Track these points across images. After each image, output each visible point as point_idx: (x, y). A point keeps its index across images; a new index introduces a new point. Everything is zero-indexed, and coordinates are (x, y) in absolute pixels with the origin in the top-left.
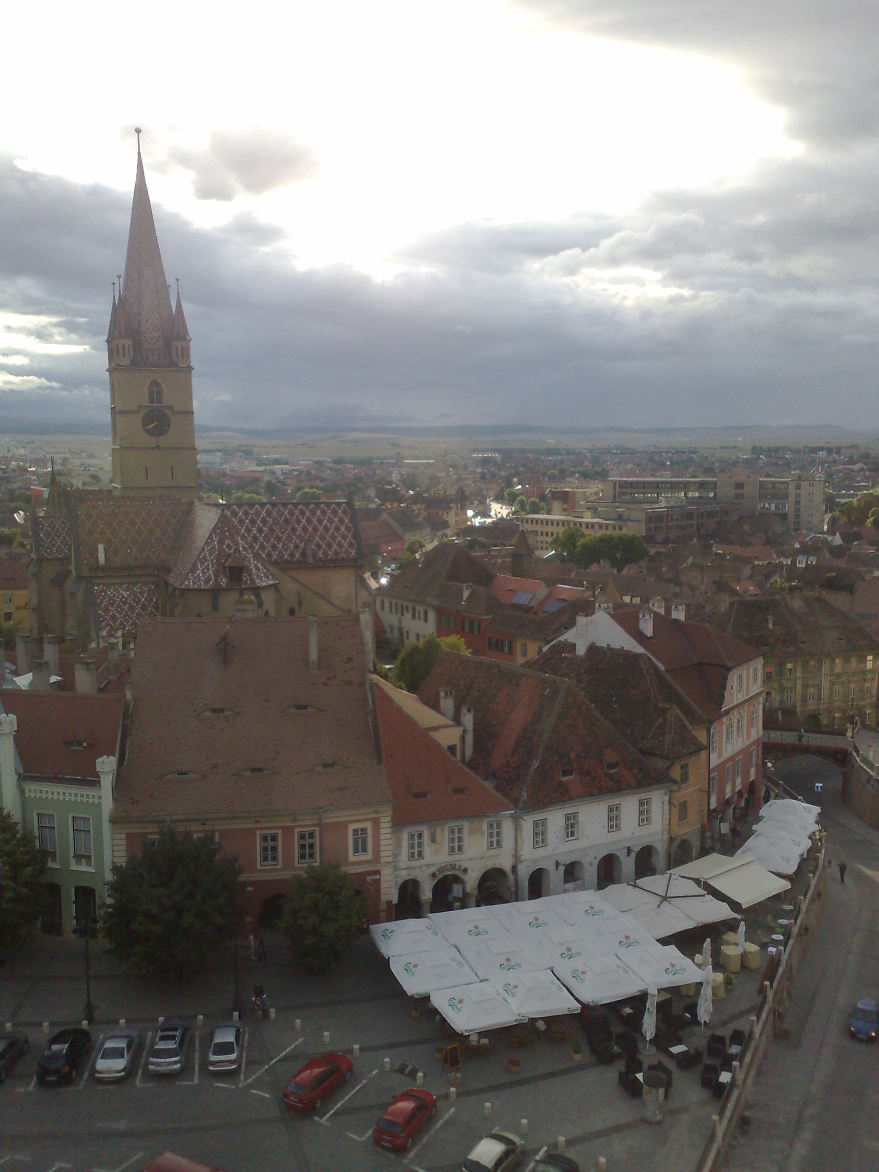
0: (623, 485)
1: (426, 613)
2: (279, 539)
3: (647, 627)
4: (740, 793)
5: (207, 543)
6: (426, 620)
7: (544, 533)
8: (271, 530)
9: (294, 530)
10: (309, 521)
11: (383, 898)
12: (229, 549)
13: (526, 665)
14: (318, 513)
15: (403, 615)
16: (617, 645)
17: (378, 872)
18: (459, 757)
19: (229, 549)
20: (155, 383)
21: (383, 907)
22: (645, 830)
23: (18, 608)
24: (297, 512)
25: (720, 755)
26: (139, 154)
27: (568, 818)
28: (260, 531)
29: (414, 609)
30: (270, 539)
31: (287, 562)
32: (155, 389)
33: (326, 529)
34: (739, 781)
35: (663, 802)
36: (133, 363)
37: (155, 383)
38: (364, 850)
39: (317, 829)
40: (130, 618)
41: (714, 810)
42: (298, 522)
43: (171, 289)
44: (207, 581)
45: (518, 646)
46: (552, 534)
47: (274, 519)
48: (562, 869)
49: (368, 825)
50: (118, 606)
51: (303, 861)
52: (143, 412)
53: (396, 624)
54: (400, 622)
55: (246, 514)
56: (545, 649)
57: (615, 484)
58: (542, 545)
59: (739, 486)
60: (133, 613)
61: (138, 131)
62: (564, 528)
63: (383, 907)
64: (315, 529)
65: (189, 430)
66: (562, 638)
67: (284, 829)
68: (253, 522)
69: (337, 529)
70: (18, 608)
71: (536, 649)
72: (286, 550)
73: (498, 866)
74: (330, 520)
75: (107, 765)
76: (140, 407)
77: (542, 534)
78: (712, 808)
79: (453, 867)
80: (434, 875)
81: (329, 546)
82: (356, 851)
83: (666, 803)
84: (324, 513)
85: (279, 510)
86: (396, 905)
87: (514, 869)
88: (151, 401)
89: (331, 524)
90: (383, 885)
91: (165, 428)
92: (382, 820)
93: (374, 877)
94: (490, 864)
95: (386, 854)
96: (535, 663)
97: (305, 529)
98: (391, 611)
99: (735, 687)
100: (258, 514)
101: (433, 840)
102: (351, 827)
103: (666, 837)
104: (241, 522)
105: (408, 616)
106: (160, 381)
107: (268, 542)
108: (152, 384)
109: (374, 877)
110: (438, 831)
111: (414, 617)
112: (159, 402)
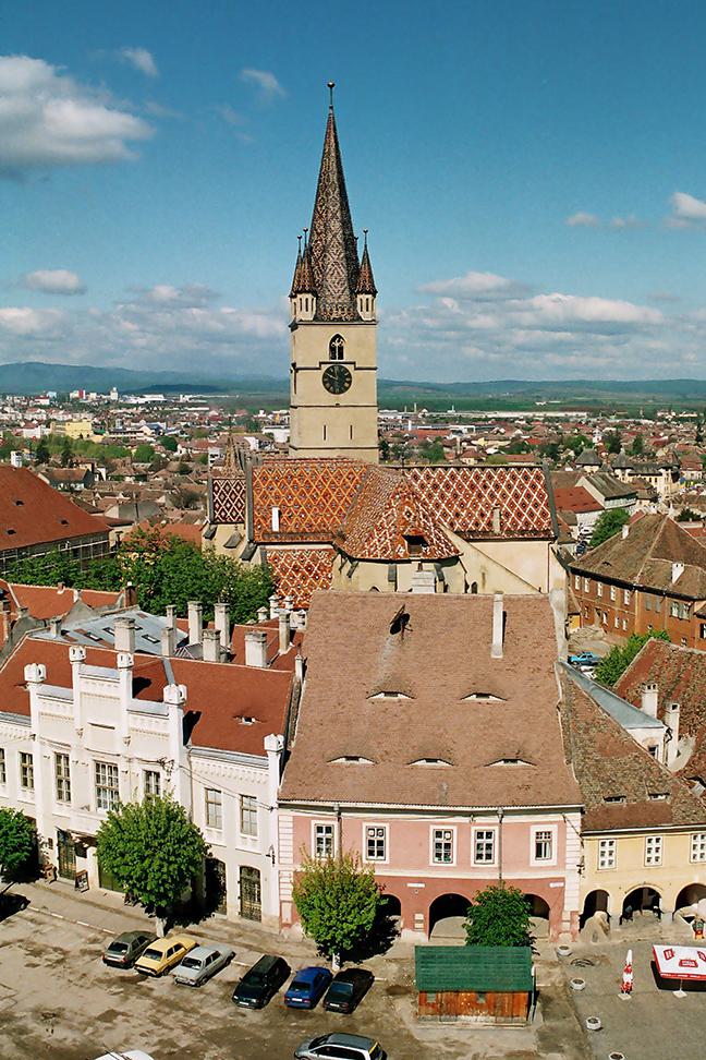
8: (455, 496)
9: (480, 496)
10: (497, 487)
12: (409, 517)
14: (508, 477)
19: (409, 517)
24: (484, 477)
28: (442, 496)
30: (453, 505)
32: (337, 345)
33: (517, 496)
36: (315, 318)
39: (497, 828)
44: (386, 548)
47: (459, 484)
50: (291, 575)
51: (479, 861)
55: (428, 477)
64: (504, 496)
67: (459, 825)
68: (435, 487)
69: (528, 496)
72: (470, 518)
74: (522, 487)
75: (273, 743)
76: (321, 363)
81: (519, 515)
82: (539, 854)
84: (514, 478)
85: (465, 475)
89: (522, 490)
91: (347, 385)
97: (492, 496)
100: (441, 477)
104: (422, 486)
108: (333, 340)
112: (341, 357)
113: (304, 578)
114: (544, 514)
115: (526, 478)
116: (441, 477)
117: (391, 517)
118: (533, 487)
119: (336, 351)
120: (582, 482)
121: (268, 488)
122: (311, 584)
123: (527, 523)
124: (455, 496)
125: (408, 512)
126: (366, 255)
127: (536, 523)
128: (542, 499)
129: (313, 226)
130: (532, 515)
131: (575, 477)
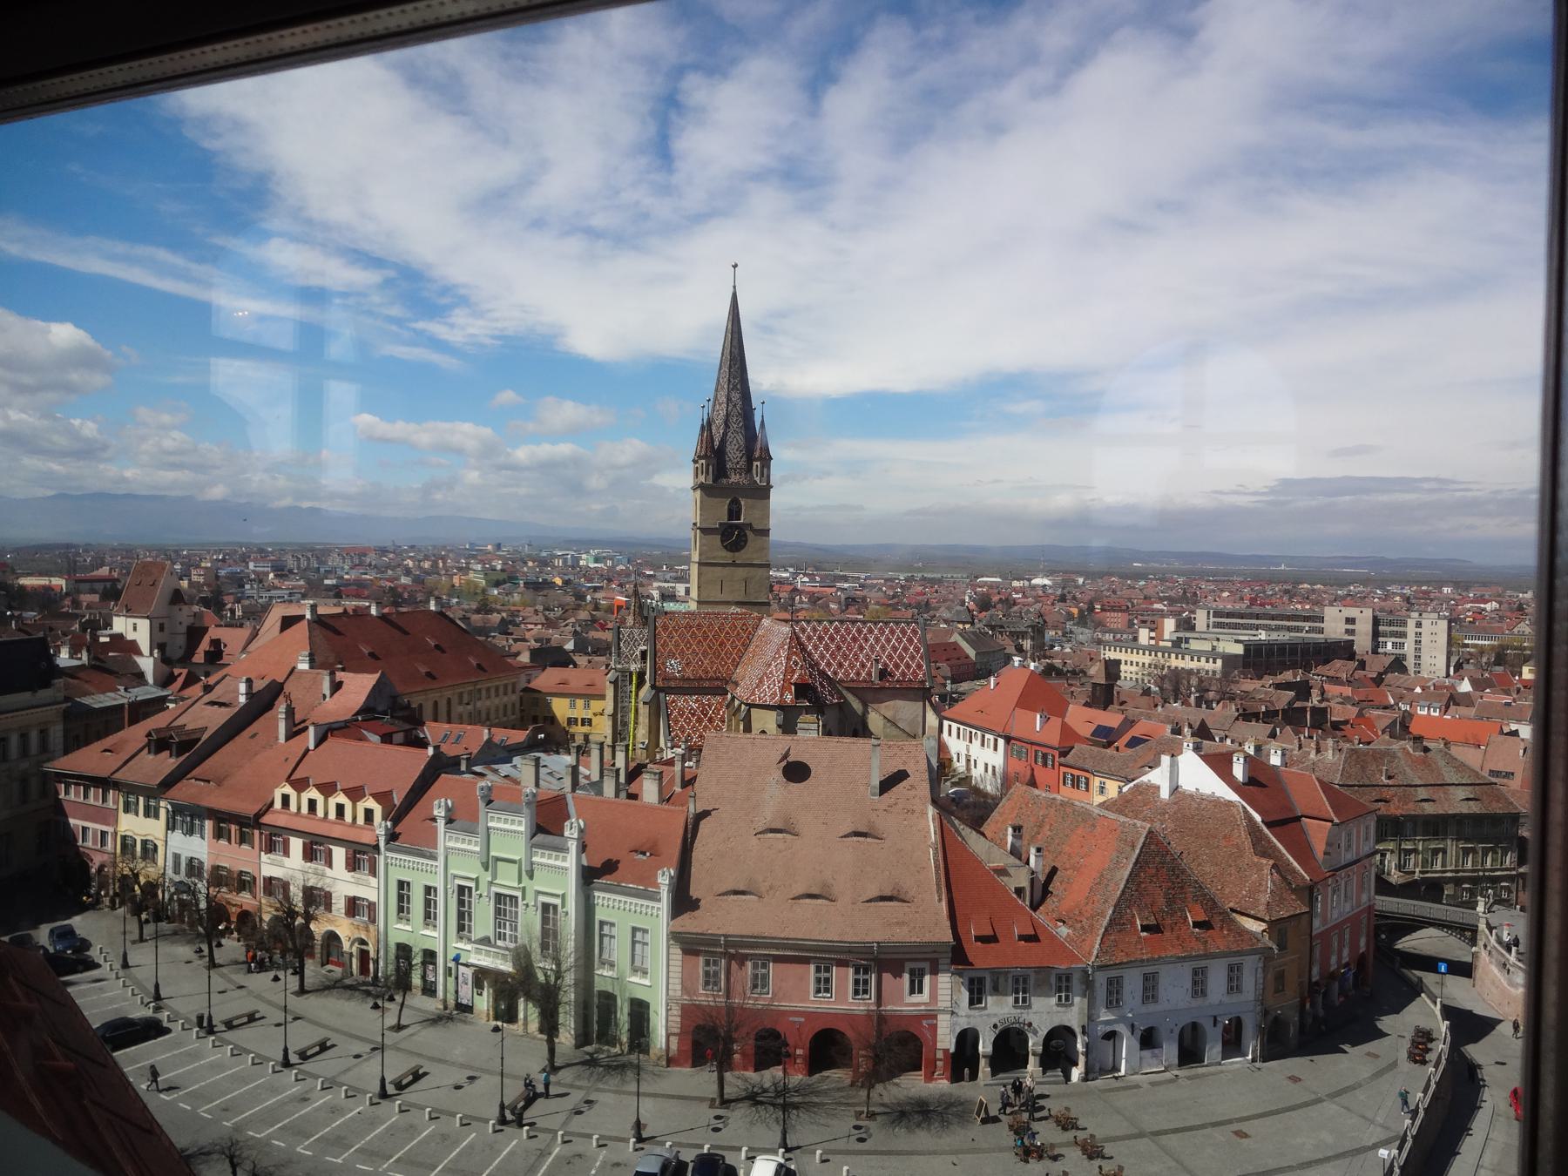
0: (1217, 614)
1: (996, 740)
2: (845, 657)
3: (1238, 771)
4: (1347, 965)
5: (774, 659)
8: (839, 648)
9: (861, 648)
11: (939, 1045)
13: (1102, 805)
15: (971, 742)
16: (1206, 790)
18: (1028, 903)
21: (940, 1055)
22: (1235, 998)
23: (595, 714)
25: (1325, 921)
26: (734, 287)
29: (983, 736)
31: (852, 681)
34: (1346, 952)
35: (1256, 970)
38: (921, 991)
40: (698, 730)
41: (1317, 983)
42: (866, 640)
44: (775, 694)
45: (1096, 782)
46: (1137, 663)
47: (842, 636)
53: (963, 752)
54: (968, 750)
55: (814, 630)
56: (1125, 789)
57: (1209, 612)
59: (1351, 621)
60: (700, 725)
61: (735, 266)
65: (764, 549)
66: (1144, 779)
68: (821, 639)
69: (905, 649)
70: (595, 714)
72: (852, 668)
74: (899, 640)
77: (1126, 664)
78: (1314, 980)
80: (995, 1026)
82: (912, 992)
83: (1260, 970)
84: (892, 632)
86: (953, 1054)
89: (900, 643)
90: (940, 1031)
92: (940, 961)
94: (1057, 1021)
98: (959, 737)
99: (1343, 845)
100: (826, 630)
103: (1259, 1009)
104: (809, 638)
105: (977, 743)
107: (834, 659)
109: (930, 1022)
111: (983, 745)
113: (699, 721)
114: (919, 666)
115: (904, 632)
116: (826, 630)
117: (779, 666)
118: (910, 641)
119: (734, 512)
120: (956, 638)
121: (668, 637)
122: (706, 727)
123: (903, 674)
124: (839, 648)
125: (795, 661)
126: (763, 422)
127: (912, 674)
128: (918, 652)
129: (716, 398)
130: (908, 666)
131: (950, 633)
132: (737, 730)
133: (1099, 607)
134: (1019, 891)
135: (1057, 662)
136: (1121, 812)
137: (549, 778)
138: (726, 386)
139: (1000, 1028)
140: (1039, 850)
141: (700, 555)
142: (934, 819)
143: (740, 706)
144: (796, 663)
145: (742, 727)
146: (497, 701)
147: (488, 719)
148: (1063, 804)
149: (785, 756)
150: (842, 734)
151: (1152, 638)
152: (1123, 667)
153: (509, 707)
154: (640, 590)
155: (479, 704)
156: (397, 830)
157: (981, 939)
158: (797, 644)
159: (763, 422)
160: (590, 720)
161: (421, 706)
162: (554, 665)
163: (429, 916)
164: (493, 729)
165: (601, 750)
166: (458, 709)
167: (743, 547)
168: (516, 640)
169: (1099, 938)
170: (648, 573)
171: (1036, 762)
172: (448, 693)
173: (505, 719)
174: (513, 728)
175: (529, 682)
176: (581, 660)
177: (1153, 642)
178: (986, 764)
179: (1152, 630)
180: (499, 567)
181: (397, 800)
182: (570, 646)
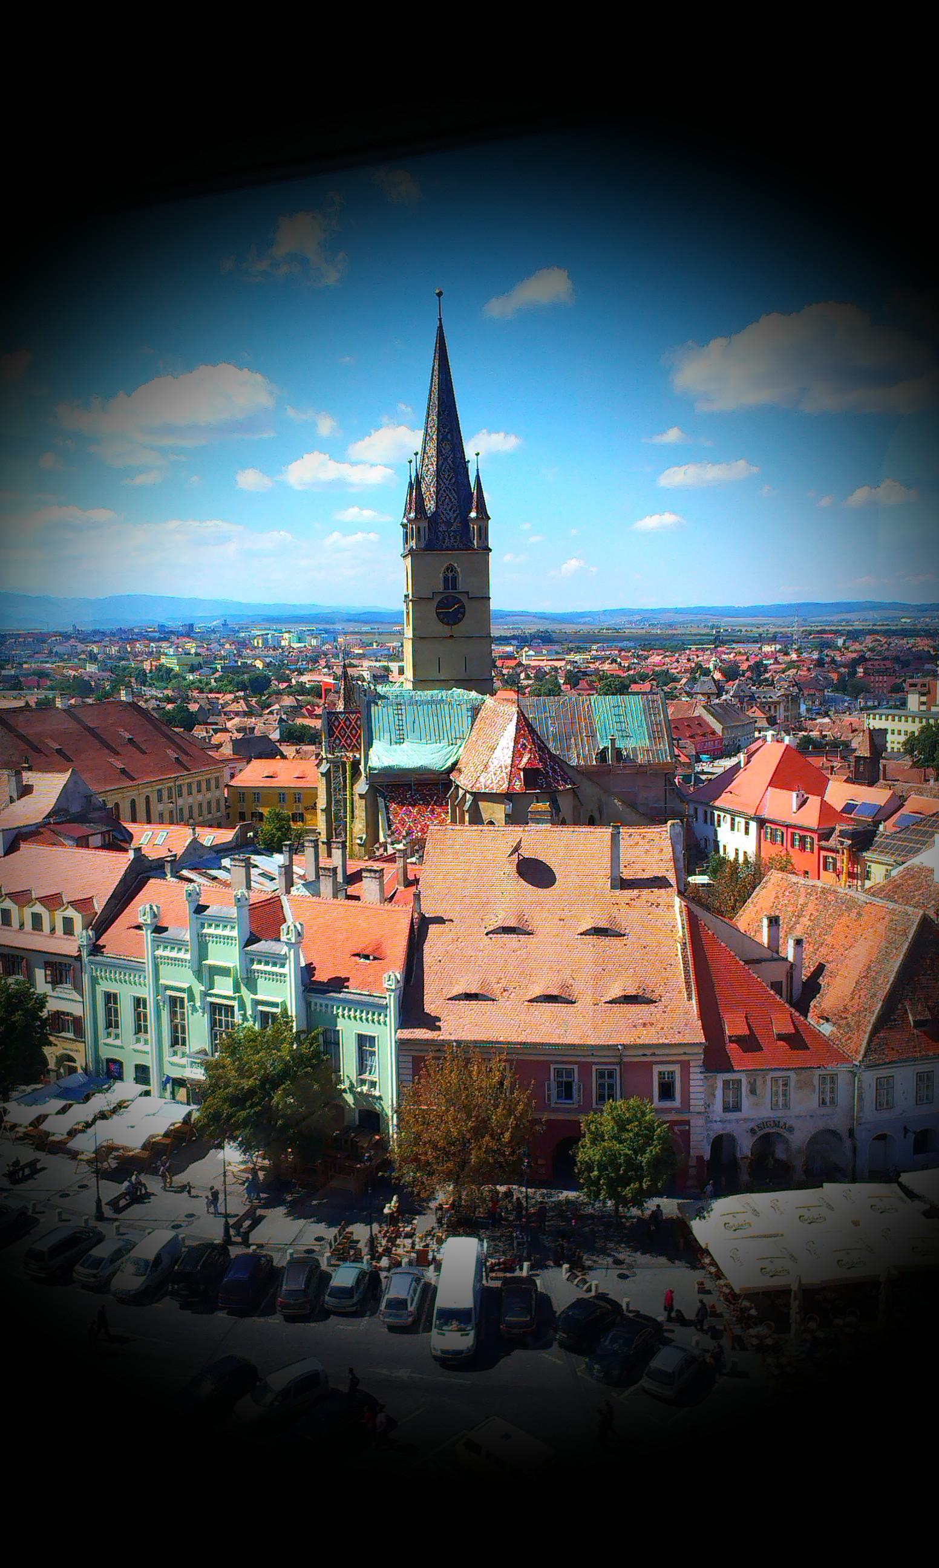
1: (747, 824)
6: (747, 832)
7: (896, 732)
11: (693, 1153)
12: (524, 749)
17: (687, 1123)
20: (450, 568)
21: (693, 1162)
23: (306, 809)
27: (920, 1077)
29: (733, 820)
32: (450, 575)
37: (450, 568)
39: (617, 1068)
43: (470, 466)
48: (911, 1137)
49: (676, 1068)
52: (438, 599)
56: (894, 873)
58: (893, 745)
62: (920, 725)
63: (693, 1162)
70: (306, 809)
71: (884, 872)
73: (832, 1127)
77: (893, 733)
79: (776, 1124)
80: (752, 1131)
87: (851, 1132)
88: (446, 587)
91: (460, 616)
93: (682, 1128)
95: (697, 1100)
96: (882, 889)
98: (706, 822)
101: (753, 1091)
102: (656, 1069)
106: (456, 565)
108: (448, 569)
109: (682, 1128)
110: (759, 1083)
111: (733, 829)
112: (454, 587)
119: (450, 581)
120: (700, 711)
126: (478, 478)
131: (692, 706)
132: (462, 821)
133: (862, 670)
134: (776, 986)
135: (815, 734)
136: (889, 898)
137: (262, 879)
138: (435, 437)
139: (760, 1133)
140: (798, 942)
141: (414, 630)
142: (681, 912)
143: (464, 795)
144: (524, 747)
145: (467, 818)
146: (200, 797)
147: (191, 817)
148: (824, 891)
149: (516, 849)
150: (576, 823)
151: (923, 703)
152: (889, 737)
153: (214, 805)
154: (350, 671)
155: (180, 801)
156: (101, 942)
157: (738, 1040)
158: (525, 727)
159: (478, 478)
160: (301, 815)
161: (117, 804)
162: (259, 757)
163: (140, 1028)
164: (198, 829)
165: (316, 847)
166: (157, 808)
167: (460, 620)
168: (216, 731)
169: (867, 1036)
170: (357, 651)
171: (793, 846)
172: (147, 791)
173: (210, 816)
174: (219, 826)
175: (232, 776)
176: (289, 750)
177: (923, 708)
178: (737, 850)
179: (923, 694)
180: (193, 651)
181: (98, 906)
182: (275, 736)
